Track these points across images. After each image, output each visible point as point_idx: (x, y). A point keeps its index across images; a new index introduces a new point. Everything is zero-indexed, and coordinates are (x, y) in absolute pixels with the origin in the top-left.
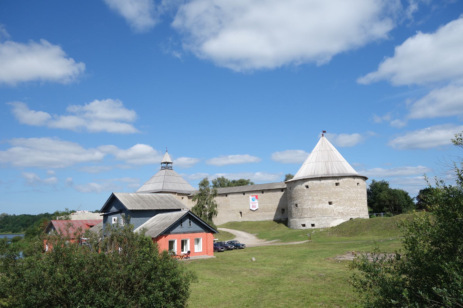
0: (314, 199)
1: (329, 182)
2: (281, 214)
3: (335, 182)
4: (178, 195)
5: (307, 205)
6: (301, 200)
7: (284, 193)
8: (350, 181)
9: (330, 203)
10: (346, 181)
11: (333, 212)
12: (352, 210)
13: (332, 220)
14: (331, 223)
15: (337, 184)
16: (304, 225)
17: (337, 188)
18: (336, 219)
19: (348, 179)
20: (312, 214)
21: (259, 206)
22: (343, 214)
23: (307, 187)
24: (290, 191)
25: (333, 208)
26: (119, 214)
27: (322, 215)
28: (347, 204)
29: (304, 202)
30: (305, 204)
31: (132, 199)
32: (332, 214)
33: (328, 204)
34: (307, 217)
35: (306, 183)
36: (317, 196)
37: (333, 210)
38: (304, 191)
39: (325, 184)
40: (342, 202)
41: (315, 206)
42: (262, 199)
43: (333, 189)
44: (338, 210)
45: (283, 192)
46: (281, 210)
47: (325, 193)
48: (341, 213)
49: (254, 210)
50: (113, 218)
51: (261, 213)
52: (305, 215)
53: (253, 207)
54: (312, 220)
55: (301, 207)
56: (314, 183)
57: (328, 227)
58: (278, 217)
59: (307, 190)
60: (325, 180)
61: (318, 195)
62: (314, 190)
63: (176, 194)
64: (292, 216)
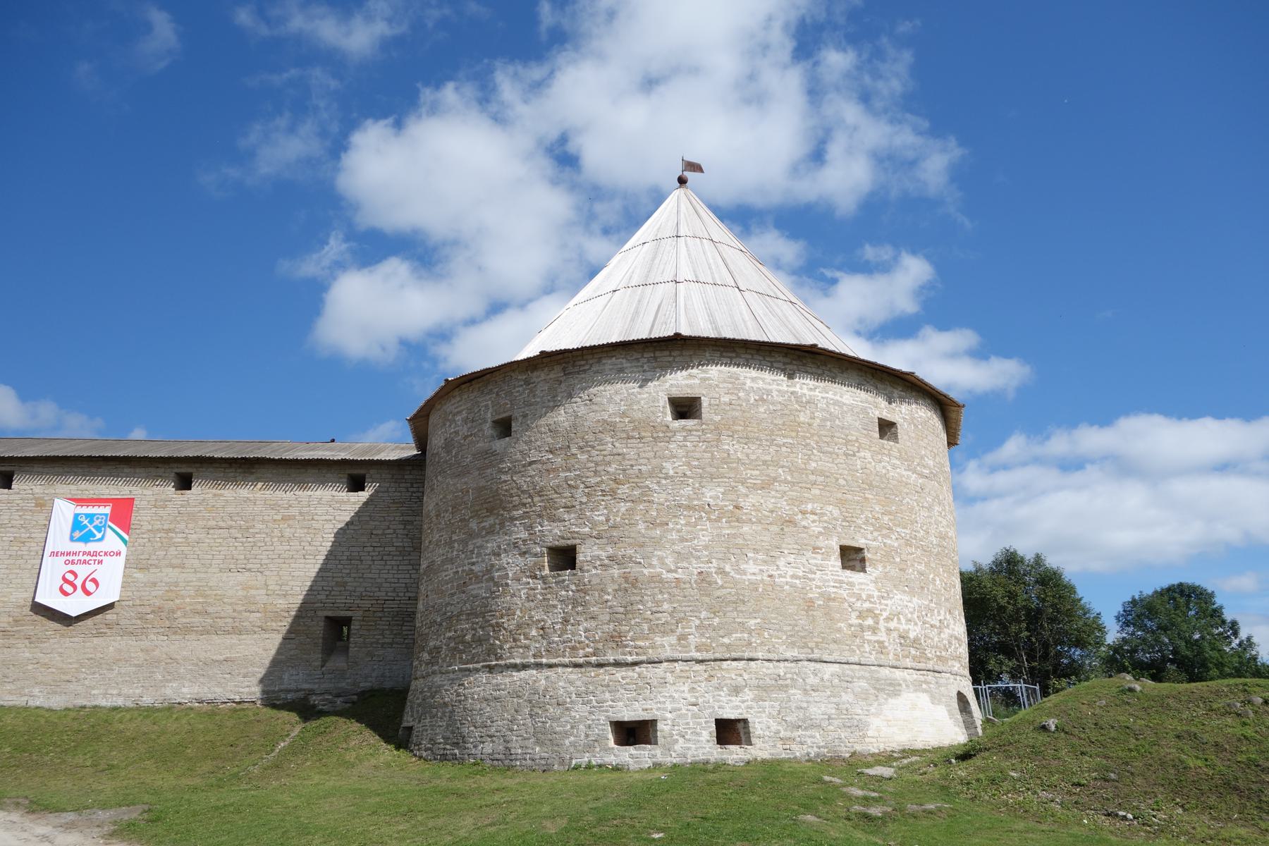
0: (747, 503)
2: (317, 657)
3: (877, 414)
6: (623, 507)
7: (366, 504)
9: (852, 557)
11: (874, 630)
13: (873, 691)
14: (875, 722)
17: (889, 455)
18: (893, 689)
20: (729, 634)
21: (125, 585)
23: (685, 408)
24: (499, 445)
25: (869, 597)
28: (934, 580)
29: (653, 524)
30: (657, 543)
32: (867, 648)
33: (835, 561)
34: (668, 653)
35: (681, 381)
36: (766, 486)
37: (869, 610)
39: (823, 410)
41: (751, 567)
42: (169, 531)
43: (868, 455)
45: (364, 496)
46: (318, 628)
47: (822, 473)
48: (916, 640)
49: (74, 614)
51: (132, 642)
52: (658, 640)
53: (68, 585)
54: (719, 688)
55: (616, 572)
57: (858, 748)
58: (286, 676)
61: (775, 479)
62: (747, 440)
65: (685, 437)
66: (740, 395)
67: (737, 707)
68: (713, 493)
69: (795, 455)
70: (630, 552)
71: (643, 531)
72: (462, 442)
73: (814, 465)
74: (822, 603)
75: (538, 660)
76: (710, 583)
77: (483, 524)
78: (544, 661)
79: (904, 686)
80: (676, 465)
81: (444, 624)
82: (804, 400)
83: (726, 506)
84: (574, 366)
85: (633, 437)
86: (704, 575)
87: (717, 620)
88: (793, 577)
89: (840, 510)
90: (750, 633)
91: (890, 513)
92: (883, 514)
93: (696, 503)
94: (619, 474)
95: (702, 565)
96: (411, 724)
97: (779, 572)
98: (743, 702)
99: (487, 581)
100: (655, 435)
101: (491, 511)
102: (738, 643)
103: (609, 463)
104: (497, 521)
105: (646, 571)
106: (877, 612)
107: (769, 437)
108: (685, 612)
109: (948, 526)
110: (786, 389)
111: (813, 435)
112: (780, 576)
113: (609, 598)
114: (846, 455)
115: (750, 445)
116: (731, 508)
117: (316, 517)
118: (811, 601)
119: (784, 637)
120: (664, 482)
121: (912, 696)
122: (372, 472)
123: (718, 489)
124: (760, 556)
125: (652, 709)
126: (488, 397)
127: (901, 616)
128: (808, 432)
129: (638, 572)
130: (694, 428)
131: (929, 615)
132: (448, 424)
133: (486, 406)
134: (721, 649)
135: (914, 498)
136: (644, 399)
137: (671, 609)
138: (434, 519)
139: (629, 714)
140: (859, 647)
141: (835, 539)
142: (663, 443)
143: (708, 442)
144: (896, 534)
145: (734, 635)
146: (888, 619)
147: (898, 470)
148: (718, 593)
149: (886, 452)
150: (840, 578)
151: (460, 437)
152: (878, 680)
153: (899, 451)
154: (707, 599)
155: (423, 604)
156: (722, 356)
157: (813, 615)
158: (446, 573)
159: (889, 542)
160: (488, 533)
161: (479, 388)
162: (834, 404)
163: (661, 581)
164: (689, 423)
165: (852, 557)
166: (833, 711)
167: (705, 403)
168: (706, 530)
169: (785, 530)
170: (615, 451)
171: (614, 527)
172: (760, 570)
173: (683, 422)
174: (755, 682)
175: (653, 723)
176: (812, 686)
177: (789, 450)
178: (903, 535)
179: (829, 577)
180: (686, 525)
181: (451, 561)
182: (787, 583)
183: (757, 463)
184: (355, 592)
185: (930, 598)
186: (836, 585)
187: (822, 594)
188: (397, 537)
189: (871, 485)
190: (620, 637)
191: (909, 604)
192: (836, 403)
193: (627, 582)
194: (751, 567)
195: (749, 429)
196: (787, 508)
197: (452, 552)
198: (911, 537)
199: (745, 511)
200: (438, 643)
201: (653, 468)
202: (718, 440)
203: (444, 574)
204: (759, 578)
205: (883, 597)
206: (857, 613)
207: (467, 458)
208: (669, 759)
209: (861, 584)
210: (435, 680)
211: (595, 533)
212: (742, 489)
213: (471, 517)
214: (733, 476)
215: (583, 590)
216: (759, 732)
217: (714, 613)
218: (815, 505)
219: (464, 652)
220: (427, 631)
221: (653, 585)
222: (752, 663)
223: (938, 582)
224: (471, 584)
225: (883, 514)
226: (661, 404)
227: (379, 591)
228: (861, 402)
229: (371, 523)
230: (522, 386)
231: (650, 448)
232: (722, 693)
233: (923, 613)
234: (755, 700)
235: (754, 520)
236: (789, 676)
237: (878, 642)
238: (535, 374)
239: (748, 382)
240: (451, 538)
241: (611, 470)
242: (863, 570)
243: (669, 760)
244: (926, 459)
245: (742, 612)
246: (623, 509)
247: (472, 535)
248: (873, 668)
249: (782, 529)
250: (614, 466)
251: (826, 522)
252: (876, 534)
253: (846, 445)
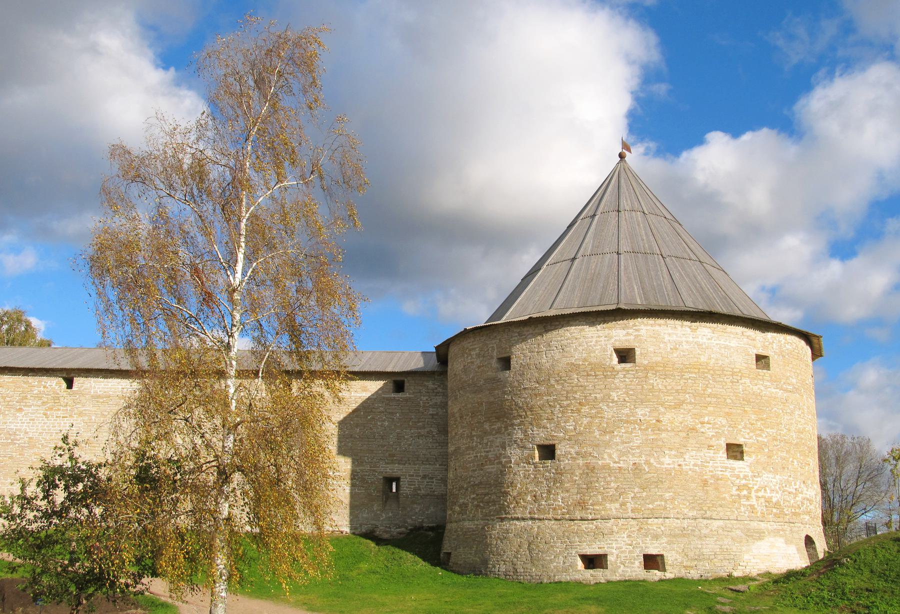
0: (665, 419)
1: (732, 345)
3: (755, 352)
5: (622, 454)
9: (735, 451)
12: (808, 496)
14: (746, 557)
15: (762, 360)
16: (593, 561)
17: (763, 379)
18: (759, 535)
22: (782, 511)
23: (625, 355)
25: (745, 477)
27: (701, 509)
28: (792, 462)
29: (604, 432)
30: (608, 445)
32: (742, 509)
33: (723, 454)
34: (614, 512)
36: (678, 405)
37: (745, 485)
38: (605, 377)
40: (777, 453)
41: (667, 460)
43: (748, 381)
44: (765, 490)
47: (715, 396)
48: (777, 503)
54: (646, 535)
55: (581, 462)
61: (683, 402)
62: (666, 376)
64: (503, 509)
65: (624, 375)
66: (661, 346)
67: (657, 547)
68: (643, 412)
69: (697, 385)
70: (590, 450)
71: (598, 436)
72: (477, 369)
73: (710, 390)
74: (713, 481)
75: (533, 515)
76: (640, 470)
77: (493, 427)
78: (536, 516)
79: (767, 533)
80: (619, 394)
81: (469, 489)
82: (704, 346)
83: (651, 420)
84: (551, 326)
85: (591, 375)
86: (637, 465)
87: (645, 494)
88: (695, 465)
89: (727, 420)
90: (666, 501)
91: (762, 419)
92: (757, 420)
93: (632, 418)
94: (582, 399)
95: (636, 459)
96: (450, 551)
97: (685, 463)
98: (661, 544)
99: (498, 463)
100: (605, 374)
101: (498, 418)
102: (658, 508)
103: (576, 392)
104: (503, 426)
105: (600, 462)
106: (750, 486)
107: (679, 374)
108: (624, 489)
109: (805, 423)
110: (691, 339)
111: (709, 370)
112: (686, 465)
113: (577, 478)
114: (732, 382)
115: (667, 380)
116: (654, 421)
117: (374, 410)
118: (706, 480)
119: (688, 504)
120: (611, 404)
121: (772, 539)
122: (409, 378)
123: (647, 409)
124: (673, 452)
125: (604, 548)
126: (493, 342)
127: (767, 488)
128: (706, 368)
129: (595, 463)
130: (631, 369)
131: (788, 486)
132: (466, 355)
133: (492, 347)
134: (647, 512)
135: (780, 408)
136: (598, 349)
137: (616, 486)
138: (459, 419)
139: (592, 550)
140: (737, 509)
141: (723, 439)
142: (610, 379)
143: (640, 378)
144: (766, 433)
145: (655, 503)
146: (757, 491)
147: (769, 389)
148: (646, 476)
149: (761, 377)
150: (726, 465)
151: (475, 366)
152: (749, 530)
153: (771, 376)
154: (638, 481)
155: (453, 474)
157: (707, 490)
158: (469, 456)
159: (760, 439)
160: (497, 433)
161: (487, 334)
162: (725, 348)
163: (610, 468)
164: (627, 366)
165: (735, 451)
166: (718, 550)
167: (638, 352)
168: (638, 436)
169: (690, 435)
170: (579, 384)
171: (580, 433)
172: (674, 462)
173: (623, 365)
174: (668, 532)
175: (605, 556)
176: (705, 534)
177: (693, 382)
178: (771, 433)
179: (719, 465)
180: (625, 433)
181: (472, 448)
182: (690, 469)
183: (671, 391)
184: (402, 461)
185: (789, 474)
186: (724, 470)
187: (713, 476)
188: (428, 424)
189: (749, 402)
190: (584, 503)
191: (773, 480)
193: (588, 469)
194: (667, 460)
195: (667, 369)
196: (691, 420)
197: (473, 443)
198: (777, 434)
199: (663, 423)
200: (466, 501)
201: (604, 396)
202: (646, 377)
203: (468, 456)
204: (672, 466)
205: (755, 476)
206: (737, 487)
207: (481, 381)
208: (615, 577)
209: (740, 468)
210: (465, 524)
211: (567, 437)
212: (662, 409)
213: (485, 421)
214: (656, 400)
215: (559, 472)
216: (670, 562)
217: (643, 489)
218: (710, 418)
219: (484, 508)
220: (457, 492)
221: (604, 471)
222: (667, 520)
223: (796, 463)
224: (487, 465)
225: (757, 420)
226: (609, 353)
227: (418, 460)
228: (744, 344)
229: (410, 414)
230: (516, 336)
231: (602, 382)
232: (648, 539)
233: (784, 485)
234: (669, 543)
235: (669, 429)
236: (690, 528)
237: (751, 505)
238: (526, 329)
239: (666, 336)
240: (471, 433)
241: (577, 396)
242: (742, 459)
243: (616, 578)
244: (791, 379)
245: (660, 488)
246: (585, 422)
247: (486, 433)
248: (746, 522)
249: (688, 434)
250: (578, 394)
251: (717, 428)
252: (751, 434)
253: (732, 375)
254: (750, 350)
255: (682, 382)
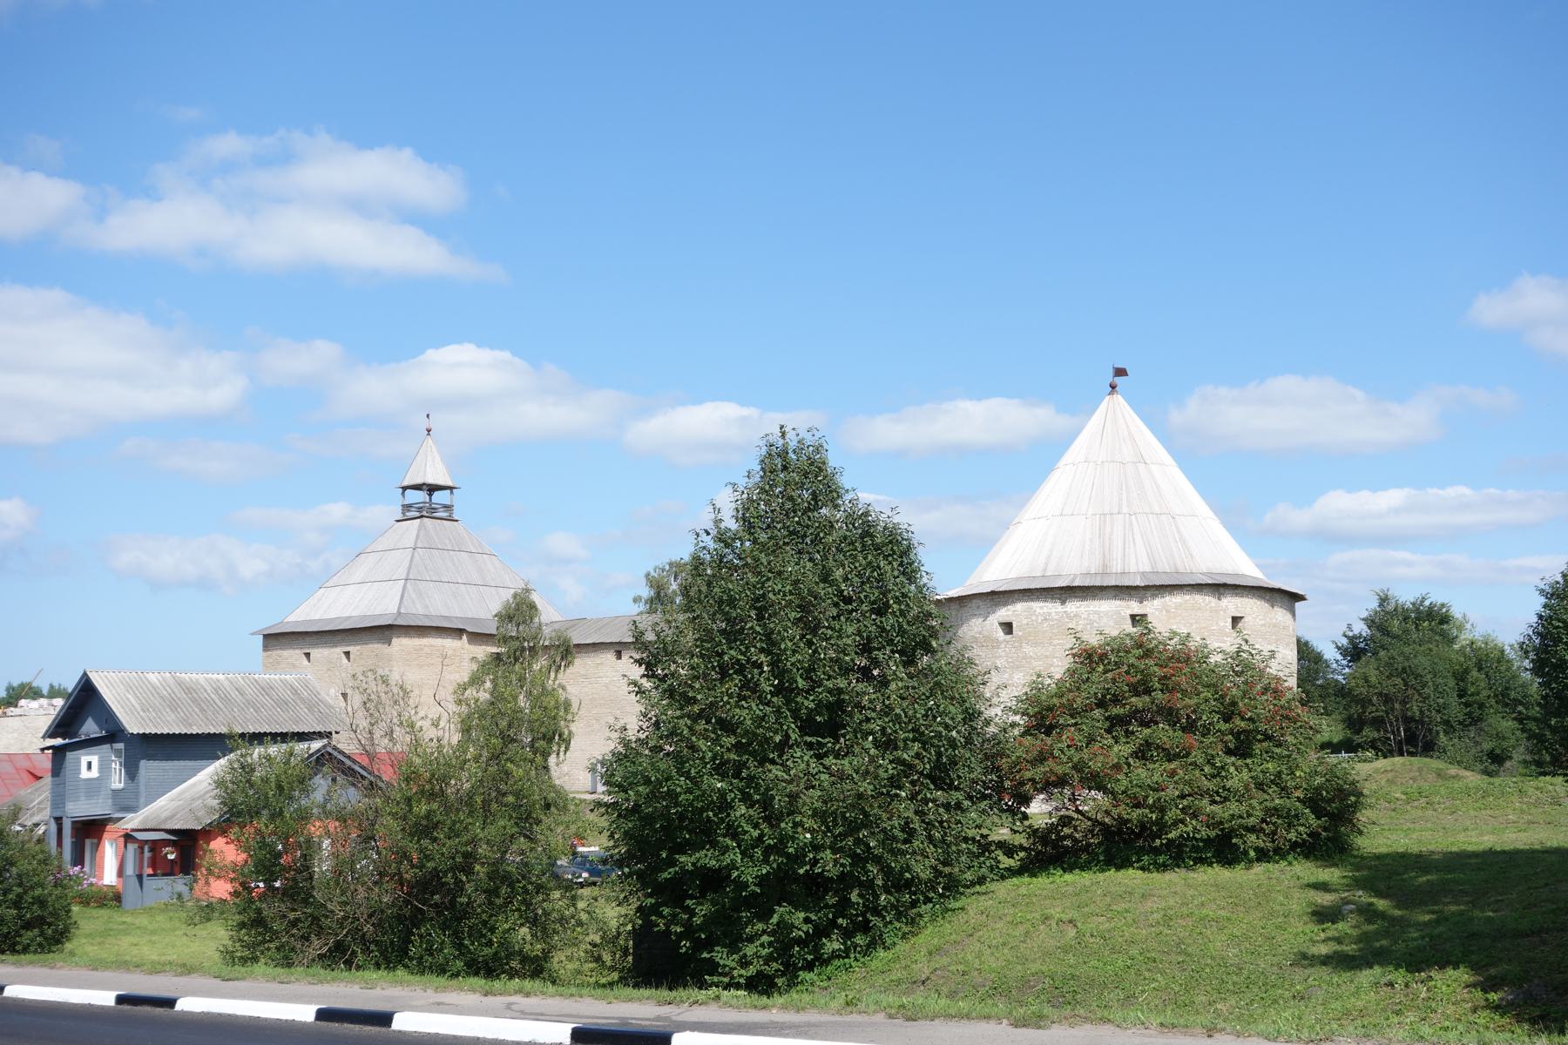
3: (1130, 612)
4: (470, 642)
8: (1199, 609)
10: (1178, 607)
19: (1188, 597)
26: (104, 746)
31: (153, 695)
35: (1004, 613)
39: (1085, 619)
50: (84, 760)
56: (1038, 610)
59: (1005, 640)
60: (1084, 598)
62: (1036, 644)
63: (465, 637)
82: (1072, 615)
85: (983, 646)
156: (1024, 596)
192: (1095, 612)
202: (1021, 646)
239: (1038, 610)
254: (1122, 612)
255: (1051, 648)
